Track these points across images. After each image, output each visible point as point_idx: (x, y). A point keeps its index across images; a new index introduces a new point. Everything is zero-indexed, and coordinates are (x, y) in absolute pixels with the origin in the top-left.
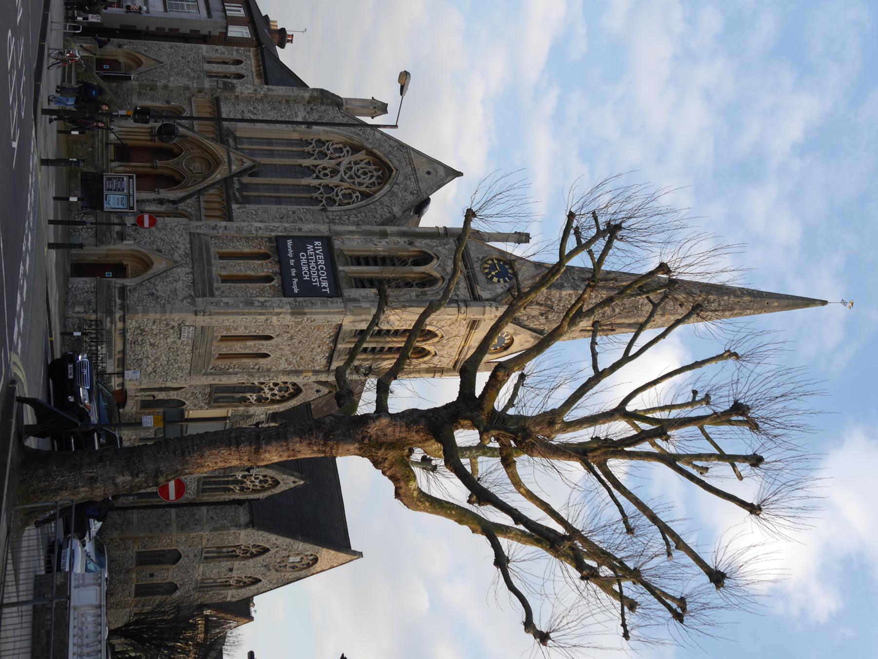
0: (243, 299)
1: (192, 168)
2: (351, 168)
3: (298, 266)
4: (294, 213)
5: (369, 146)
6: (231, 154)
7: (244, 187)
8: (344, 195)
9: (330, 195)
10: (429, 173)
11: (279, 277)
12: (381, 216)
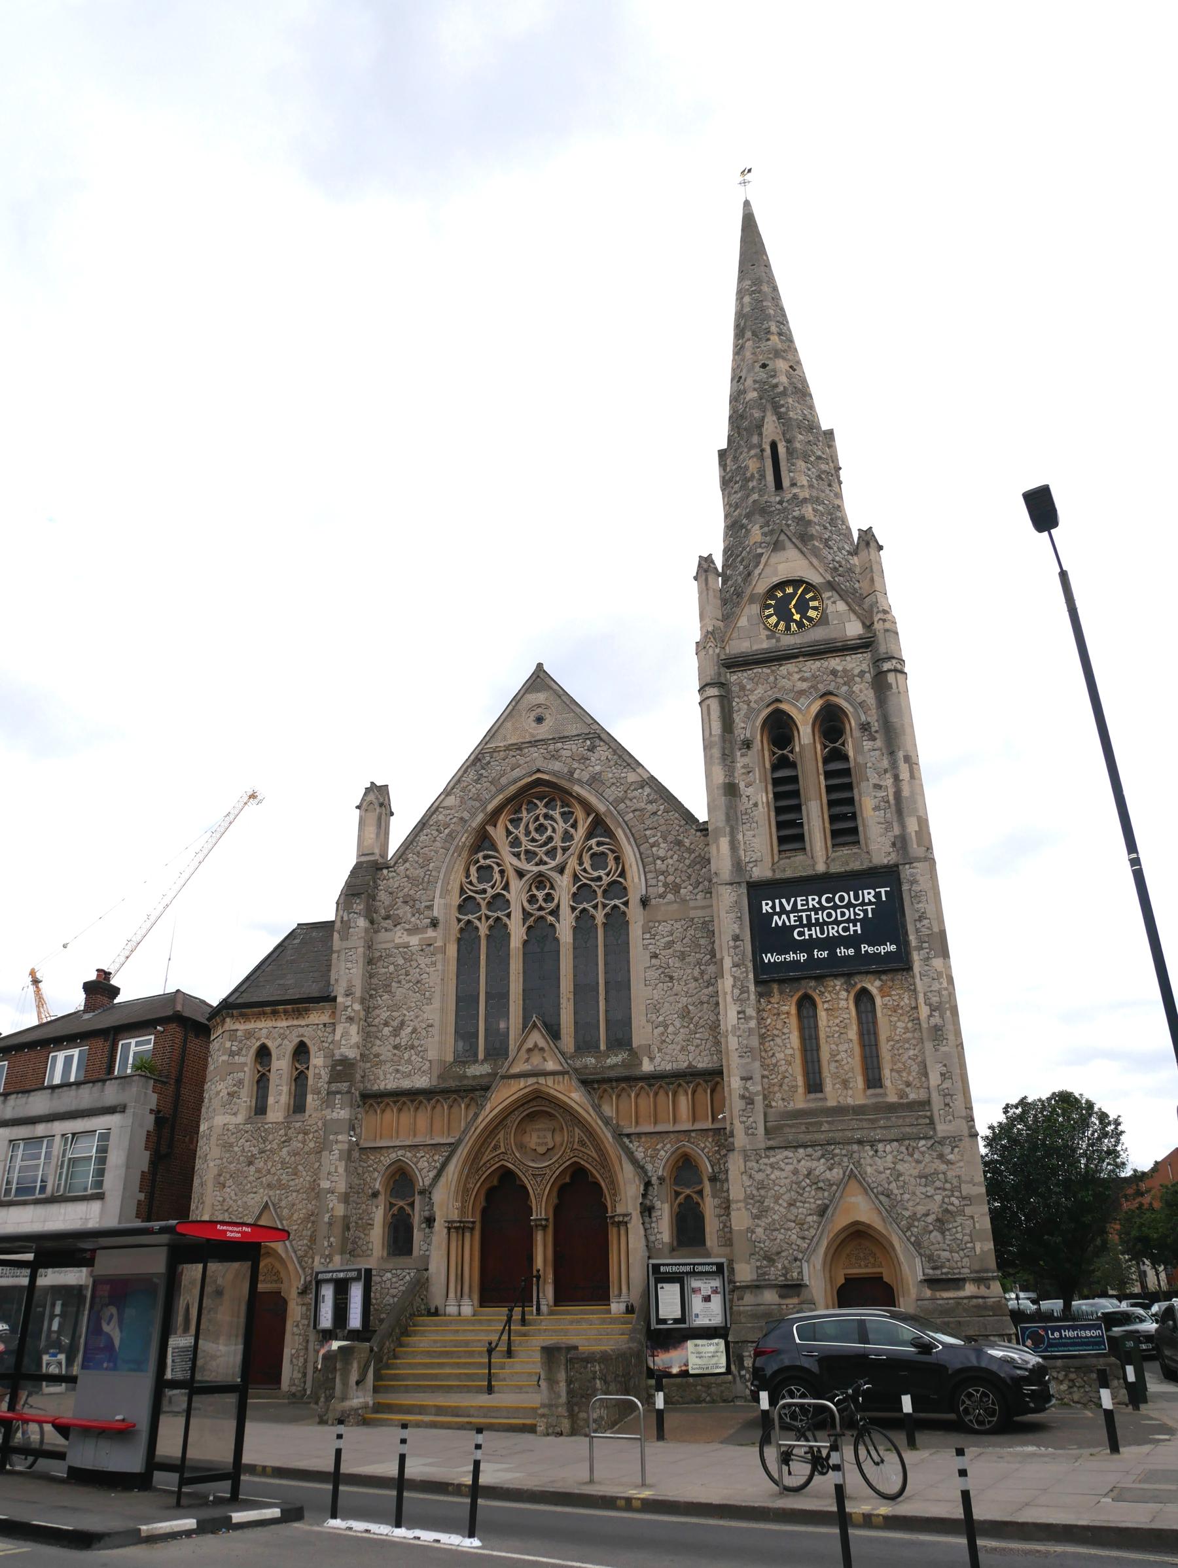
0: (929, 1046)
1: (542, 1150)
2: (527, 852)
3: (831, 943)
4: (655, 956)
5: (480, 817)
6: (515, 1070)
7: (586, 1044)
8: (595, 867)
9: (599, 892)
10: (539, 720)
11: (857, 979)
12: (651, 802)
